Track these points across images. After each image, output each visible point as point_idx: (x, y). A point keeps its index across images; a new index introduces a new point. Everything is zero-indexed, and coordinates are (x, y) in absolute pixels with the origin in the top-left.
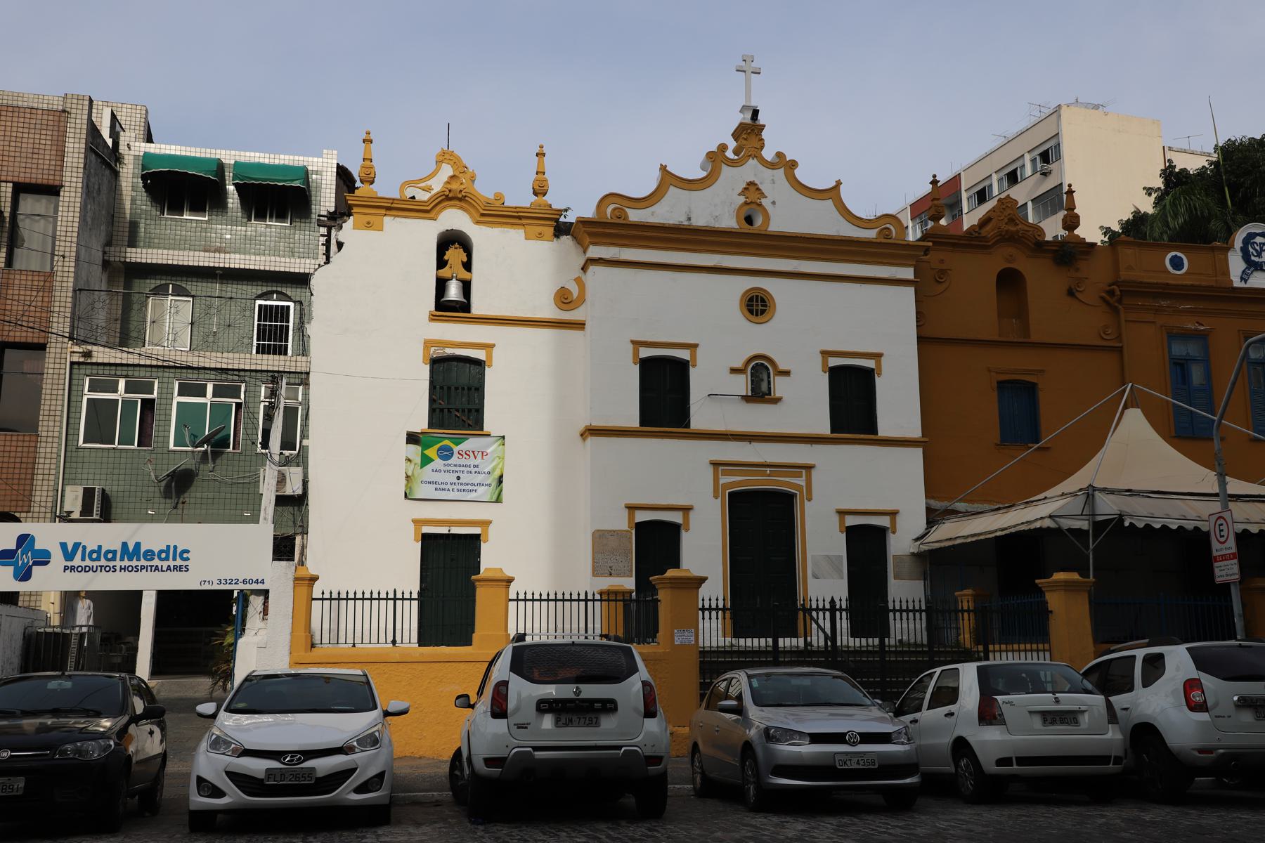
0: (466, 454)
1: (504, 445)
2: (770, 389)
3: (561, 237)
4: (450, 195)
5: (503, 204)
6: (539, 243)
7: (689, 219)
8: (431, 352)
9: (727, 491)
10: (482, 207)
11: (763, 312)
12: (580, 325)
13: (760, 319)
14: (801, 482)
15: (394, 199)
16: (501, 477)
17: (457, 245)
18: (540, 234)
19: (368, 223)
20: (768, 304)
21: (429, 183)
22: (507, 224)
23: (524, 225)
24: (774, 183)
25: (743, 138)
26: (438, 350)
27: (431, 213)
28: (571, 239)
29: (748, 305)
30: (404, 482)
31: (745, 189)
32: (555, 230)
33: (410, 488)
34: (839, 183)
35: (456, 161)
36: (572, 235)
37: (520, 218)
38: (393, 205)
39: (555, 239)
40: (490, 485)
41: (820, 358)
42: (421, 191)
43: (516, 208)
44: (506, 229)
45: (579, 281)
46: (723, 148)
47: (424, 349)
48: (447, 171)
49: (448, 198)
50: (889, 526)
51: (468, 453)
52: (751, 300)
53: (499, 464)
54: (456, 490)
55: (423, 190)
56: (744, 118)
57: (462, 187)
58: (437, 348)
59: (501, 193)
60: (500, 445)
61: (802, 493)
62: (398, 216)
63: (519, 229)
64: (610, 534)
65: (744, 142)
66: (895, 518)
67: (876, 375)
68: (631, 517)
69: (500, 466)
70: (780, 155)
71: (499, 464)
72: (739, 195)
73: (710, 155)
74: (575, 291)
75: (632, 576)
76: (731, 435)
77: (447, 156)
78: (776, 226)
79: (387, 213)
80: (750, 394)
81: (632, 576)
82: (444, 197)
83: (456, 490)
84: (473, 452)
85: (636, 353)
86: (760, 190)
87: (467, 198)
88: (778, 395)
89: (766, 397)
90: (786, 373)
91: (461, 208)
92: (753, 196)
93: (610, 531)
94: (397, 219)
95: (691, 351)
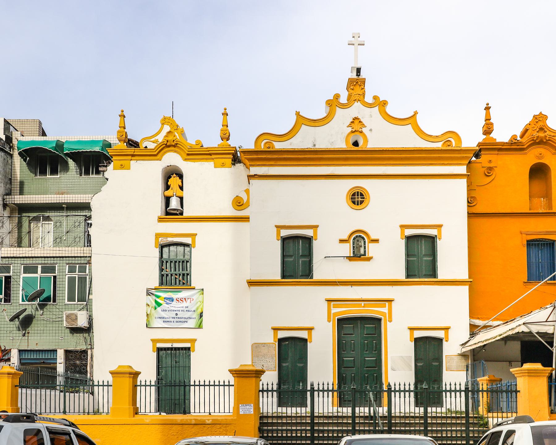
0: (181, 300)
1: (203, 294)
2: (365, 251)
3: (236, 165)
4: (168, 144)
5: (202, 146)
6: (223, 169)
7: (315, 145)
9: (336, 318)
11: (362, 202)
12: (246, 219)
13: (360, 207)
14: (385, 310)
16: (201, 313)
17: (174, 175)
18: (223, 164)
19: (122, 165)
20: (365, 196)
21: (156, 138)
22: (203, 159)
23: (213, 159)
24: (371, 117)
25: (351, 88)
26: (163, 239)
27: (158, 156)
28: (243, 166)
29: (352, 198)
30: (146, 318)
31: (351, 122)
32: (232, 160)
33: (149, 321)
34: (416, 113)
36: (243, 163)
37: (210, 154)
38: (135, 153)
39: (233, 166)
40: (195, 318)
41: (399, 230)
42: (152, 143)
43: (207, 148)
44: (202, 162)
45: (247, 191)
46: (337, 96)
48: (167, 128)
49: (167, 146)
50: (444, 337)
51: (182, 299)
52: (354, 195)
54: (175, 322)
55: (153, 143)
56: (352, 76)
57: (175, 138)
58: (163, 238)
59: (200, 141)
60: (200, 294)
61: (385, 317)
63: (211, 162)
65: (351, 91)
66: (448, 332)
67: (438, 239)
68: (275, 335)
69: (201, 307)
70: (375, 98)
72: (348, 126)
73: (329, 103)
74: (244, 197)
76: (338, 282)
77: (167, 120)
78: (372, 144)
79: (132, 159)
80: (352, 255)
82: (164, 145)
83: (175, 322)
84: (185, 299)
85: (278, 233)
86: (361, 122)
87: (178, 145)
88: (370, 255)
89: (362, 257)
90: (376, 241)
91: (175, 151)
92: (356, 127)
93: (263, 344)
94: (138, 162)
95: (314, 231)
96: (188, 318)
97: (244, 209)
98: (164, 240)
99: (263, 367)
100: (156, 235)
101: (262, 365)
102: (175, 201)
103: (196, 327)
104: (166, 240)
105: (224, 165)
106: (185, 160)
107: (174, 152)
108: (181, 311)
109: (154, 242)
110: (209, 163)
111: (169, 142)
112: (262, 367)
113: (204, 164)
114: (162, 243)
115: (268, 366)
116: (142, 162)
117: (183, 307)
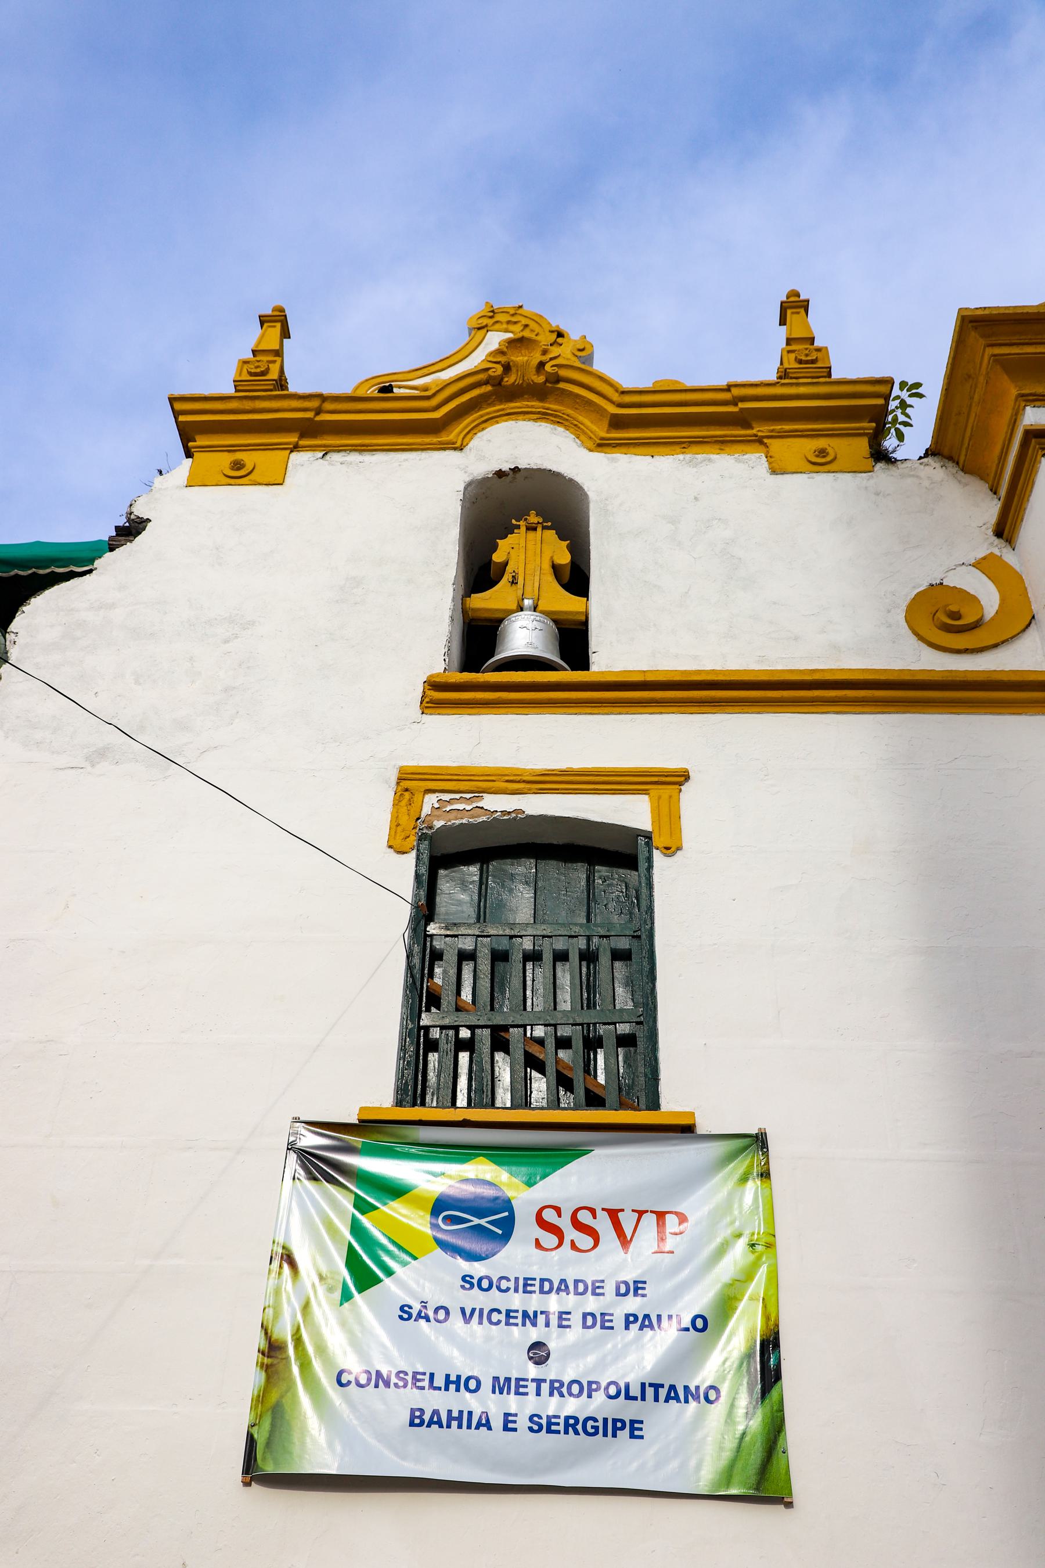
0: (578, 1225)
6: (823, 482)
8: (426, 810)
10: (616, 397)
15: (322, 398)
16: (770, 1343)
17: (533, 518)
35: (528, 322)
43: (729, 388)
47: (396, 804)
48: (494, 340)
51: (584, 1217)
53: (747, 1275)
54: (522, 1423)
58: (446, 797)
62: (338, 449)
69: (757, 1285)
71: (747, 1275)
82: (488, 388)
84: (613, 1214)
91: (544, 416)
96: (650, 1392)
97: (995, 646)
98: (460, 806)
100: (400, 780)
102: (531, 626)
103: (728, 1484)
104: (468, 808)
105: (829, 459)
106: (600, 449)
107: (535, 420)
108: (576, 1319)
109: (388, 817)
110: (736, 455)
111: (514, 370)
113: (710, 460)
114: (438, 824)
116: (354, 457)
117: (597, 1289)
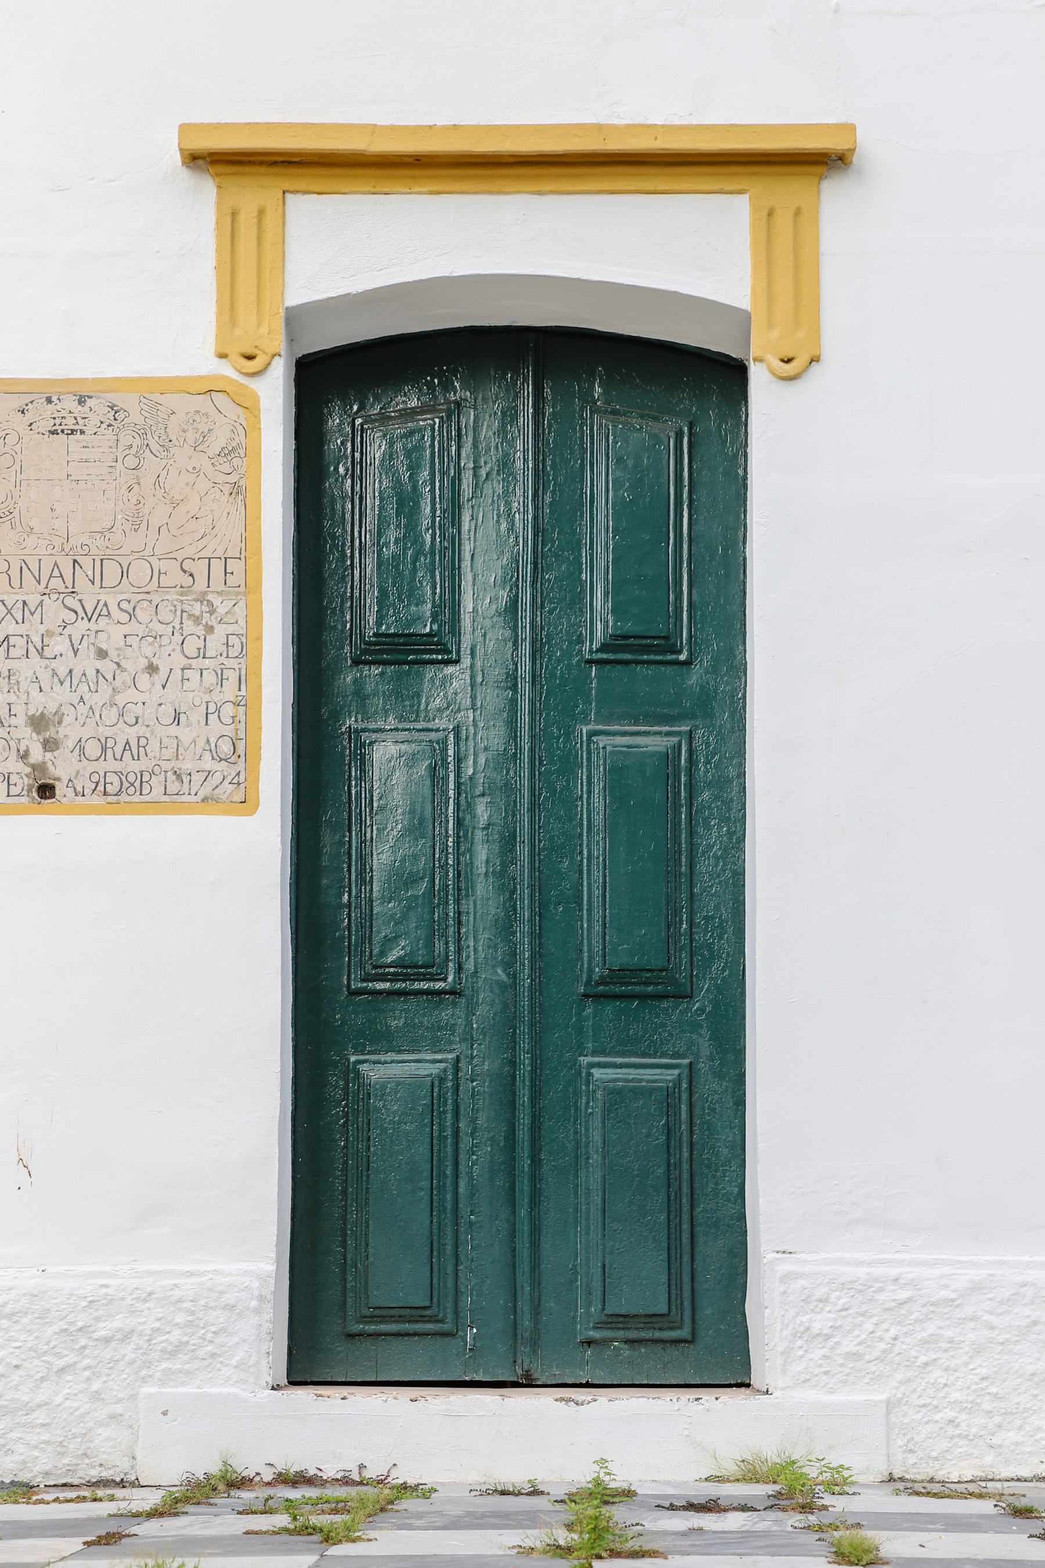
64: (44, 416)
75: (247, 804)
81: (247, 804)
99: (50, 745)
101: (38, 723)
112: (37, 754)
115: (132, 733)
